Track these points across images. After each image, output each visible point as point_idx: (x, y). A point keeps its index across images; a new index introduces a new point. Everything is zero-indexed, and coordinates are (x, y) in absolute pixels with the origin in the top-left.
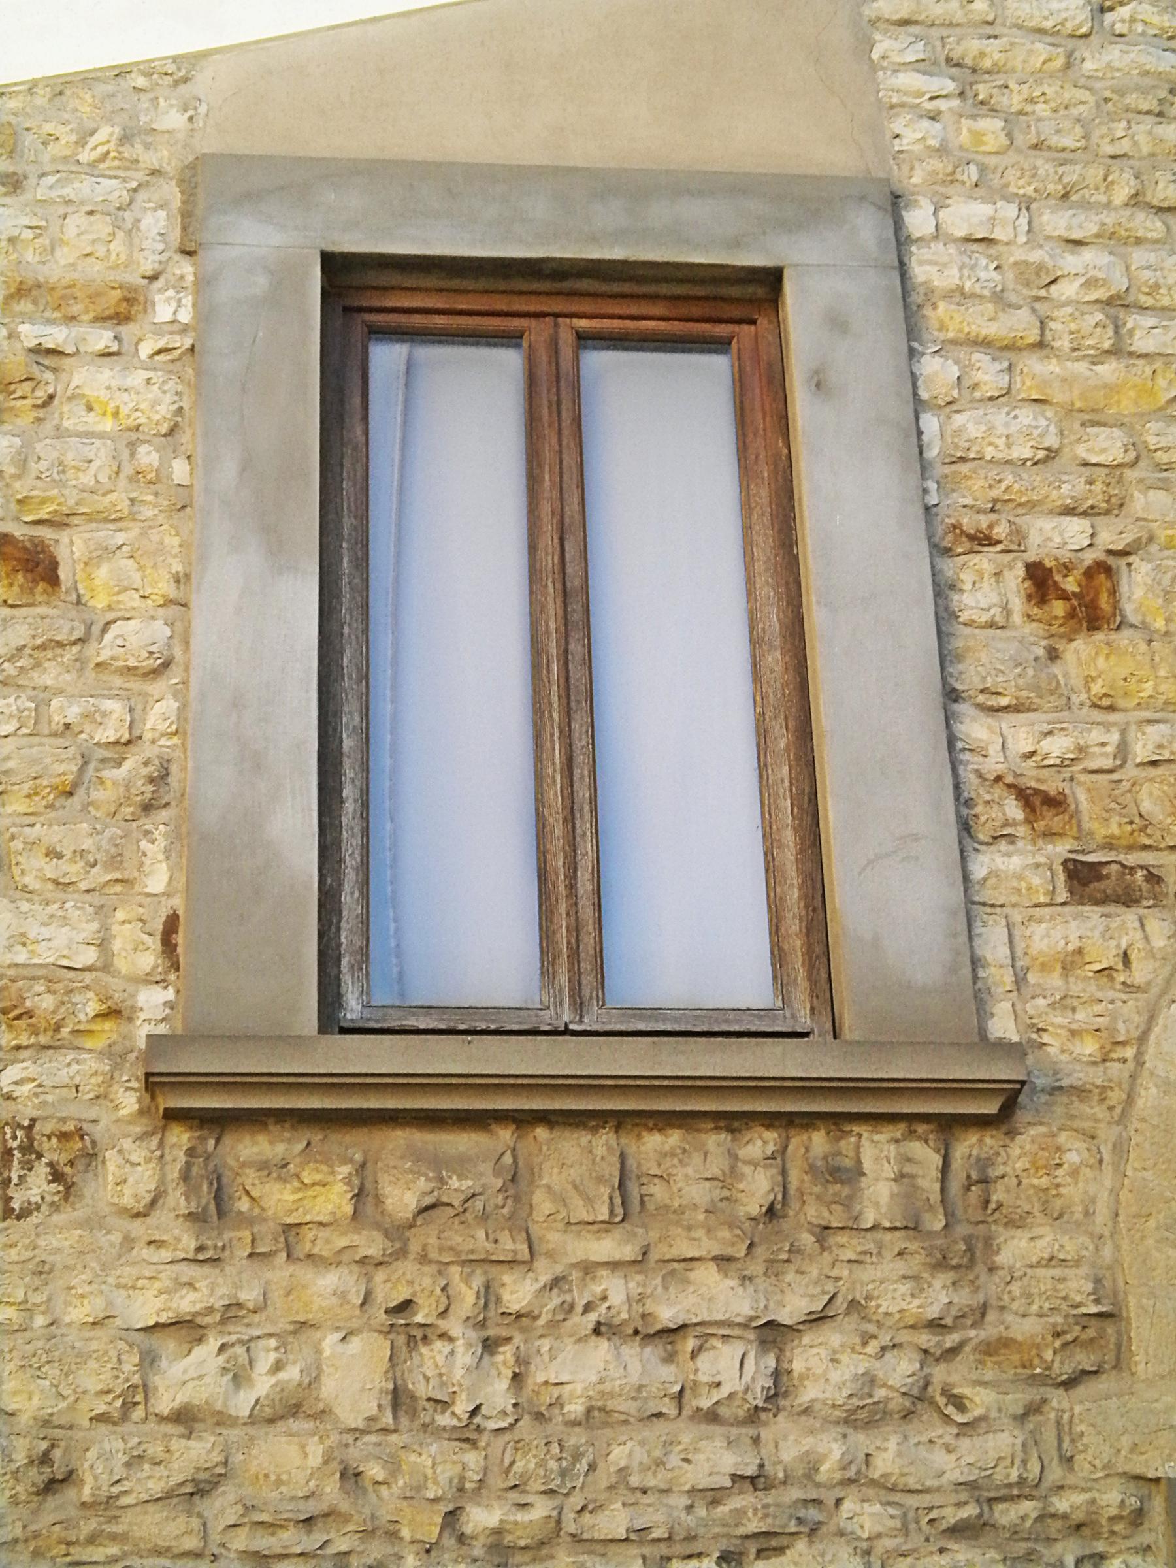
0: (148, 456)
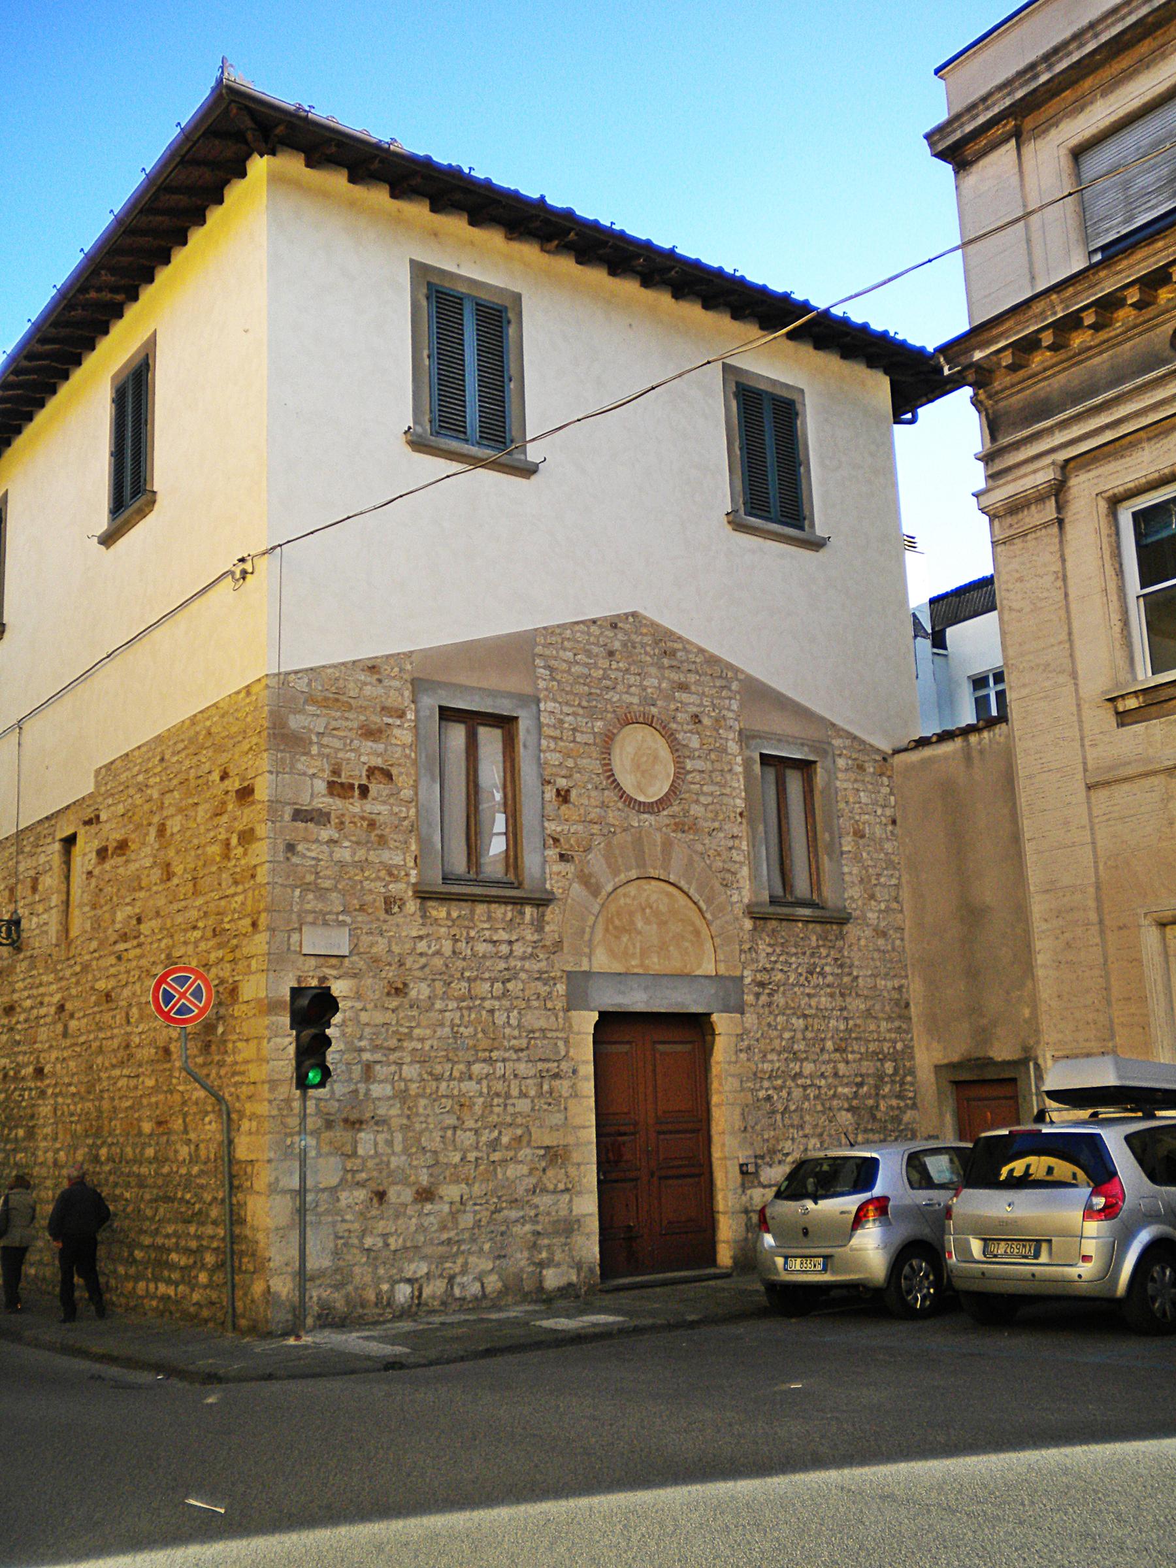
0: (407, 751)
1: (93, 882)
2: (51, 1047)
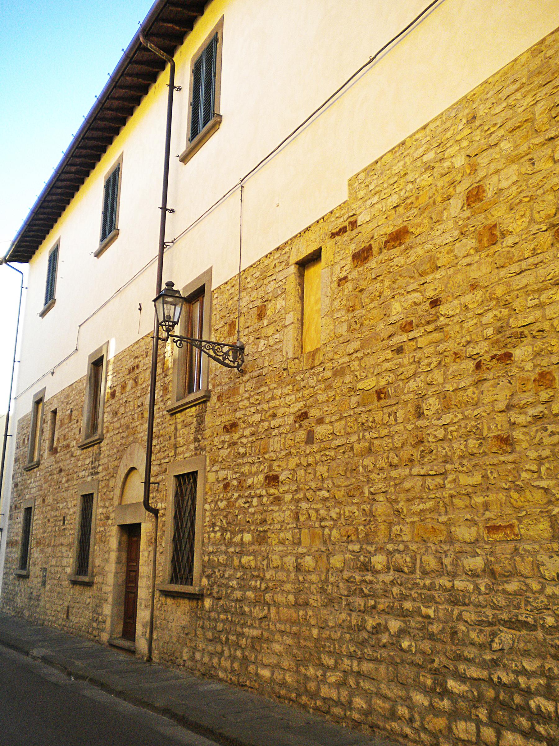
1: (349, 286)
2: (290, 454)
